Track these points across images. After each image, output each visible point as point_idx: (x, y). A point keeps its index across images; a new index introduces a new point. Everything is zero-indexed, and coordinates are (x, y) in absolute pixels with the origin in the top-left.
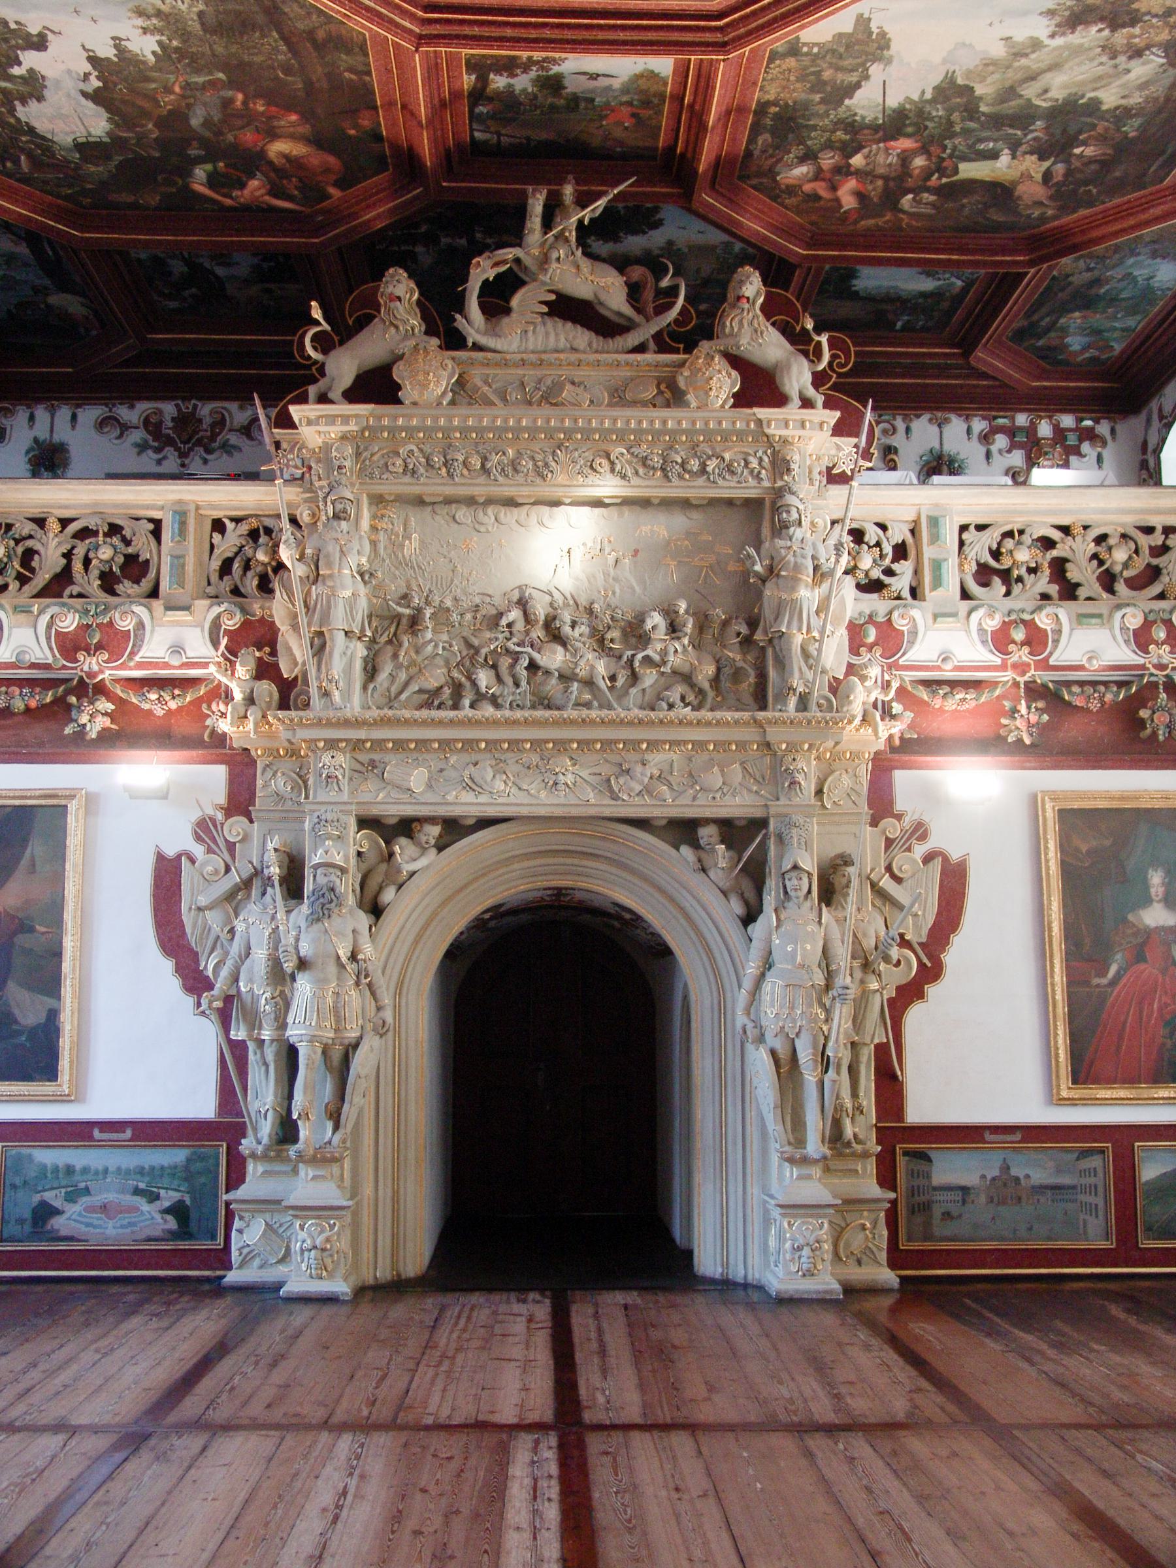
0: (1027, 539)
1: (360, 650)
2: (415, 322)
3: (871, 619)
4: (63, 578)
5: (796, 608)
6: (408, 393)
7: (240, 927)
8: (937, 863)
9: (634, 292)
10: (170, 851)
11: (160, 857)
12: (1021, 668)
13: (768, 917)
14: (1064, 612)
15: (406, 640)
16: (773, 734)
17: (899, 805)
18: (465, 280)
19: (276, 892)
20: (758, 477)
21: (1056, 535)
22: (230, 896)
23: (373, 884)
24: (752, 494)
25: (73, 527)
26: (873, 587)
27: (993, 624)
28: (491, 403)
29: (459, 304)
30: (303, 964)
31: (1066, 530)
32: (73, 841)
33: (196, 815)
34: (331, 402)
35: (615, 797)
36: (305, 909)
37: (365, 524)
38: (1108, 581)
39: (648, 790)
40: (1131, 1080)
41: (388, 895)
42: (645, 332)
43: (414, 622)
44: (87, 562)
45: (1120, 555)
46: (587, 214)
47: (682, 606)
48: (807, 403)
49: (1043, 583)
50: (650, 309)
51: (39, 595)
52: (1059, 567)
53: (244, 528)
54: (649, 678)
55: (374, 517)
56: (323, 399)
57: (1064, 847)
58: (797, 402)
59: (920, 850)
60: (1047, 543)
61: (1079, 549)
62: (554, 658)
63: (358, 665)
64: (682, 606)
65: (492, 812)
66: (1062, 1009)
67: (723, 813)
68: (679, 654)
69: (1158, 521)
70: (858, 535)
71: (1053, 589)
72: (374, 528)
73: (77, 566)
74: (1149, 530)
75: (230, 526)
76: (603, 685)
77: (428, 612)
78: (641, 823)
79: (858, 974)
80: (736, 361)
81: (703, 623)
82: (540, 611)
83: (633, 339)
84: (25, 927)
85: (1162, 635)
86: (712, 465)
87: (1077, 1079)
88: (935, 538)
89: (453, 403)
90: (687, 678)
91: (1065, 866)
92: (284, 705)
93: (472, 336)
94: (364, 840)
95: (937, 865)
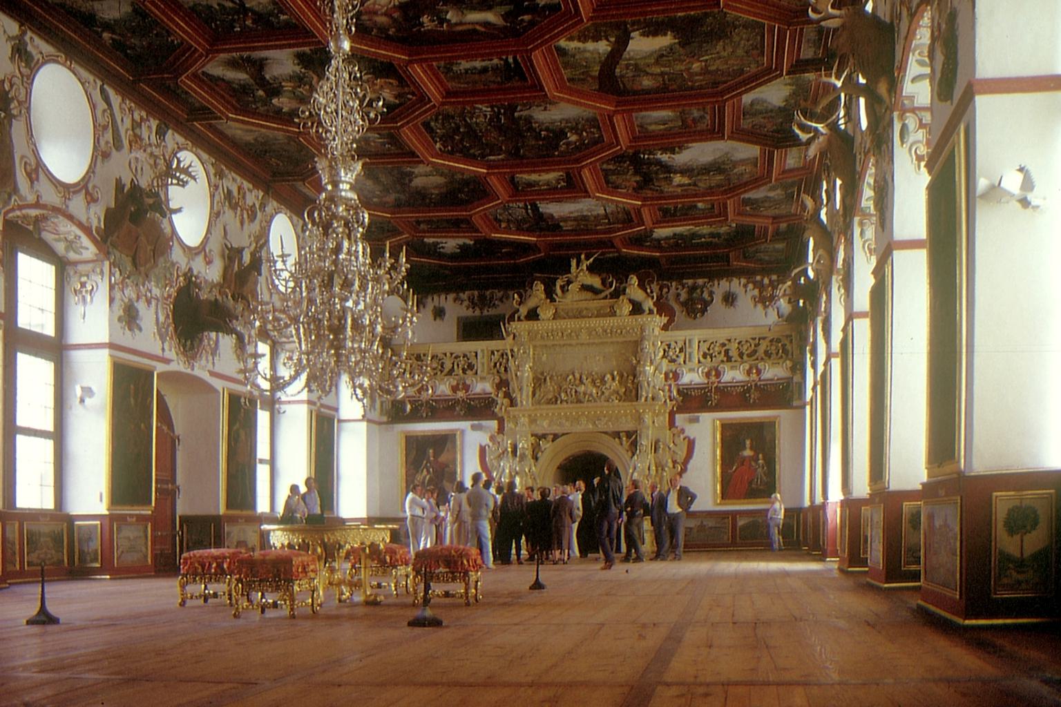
0: (718, 344)
1: (531, 389)
2: (543, 296)
3: (671, 371)
4: (452, 370)
5: (645, 372)
6: (542, 316)
7: (502, 464)
8: (687, 440)
9: (603, 283)
10: (483, 444)
11: (481, 446)
12: (713, 383)
13: (636, 457)
14: (726, 367)
15: (543, 386)
16: (637, 408)
17: (677, 424)
18: (555, 285)
19: (510, 454)
20: (636, 333)
21: (727, 342)
22: (499, 456)
23: (536, 450)
24: (636, 339)
25: (454, 356)
26: (673, 361)
27: (706, 370)
28: (565, 318)
29: (554, 292)
30: (517, 473)
31: (729, 340)
32: (458, 443)
33: (489, 434)
34: (521, 321)
35: (597, 426)
36: (518, 459)
37: (531, 353)
38: (741, 355)
39: (606, 424)
40: (739, 498)
41: (540, 454)
42: (607, 292)
43: (545, 380)
44: (458, 365)
45: (745, 347)
46: (588, 263)
47: (616, 373)
48: (651, 312)
49: (722, 357)
50: (608, 285)
51: (446, 375)
52: (727, 352)
53: (500, 353)
54: (607, 393)
55: (534, 350)
56: (519, 319)
57: (722, 434)
58: (648, 312)
59: (682, 437)
60: (723, 345)
61: (733, 347)
62: (582, 389)
63: (530, 393)
64: (616, 373)
65: (565, 432)
66: (719, 479)
67: (626, 429)
68: (615, 385)
69: (757, 337)
70: (669, 346)
71: (725, 359)
72: (534, 354)
73: (456, 367)
74: (754, 339)
75: (496, 353)
76: (595, 395)
77: (548, 378)
78: (606, 433)
79: (660, 471)
80: (631, 301)
81: (621, 376)
82: (577, 376)
83: (603, 295)
84: (447, 466)
85: (754, 371)
86: (624, 331)
87: (723, 498)
88: (690, 346)
89: (553, 319)
90: (618, 393)
91: (722, 439)
92: (512, 405)
93: (557, 300)
94: (532, 439)
95: (687, 440)
